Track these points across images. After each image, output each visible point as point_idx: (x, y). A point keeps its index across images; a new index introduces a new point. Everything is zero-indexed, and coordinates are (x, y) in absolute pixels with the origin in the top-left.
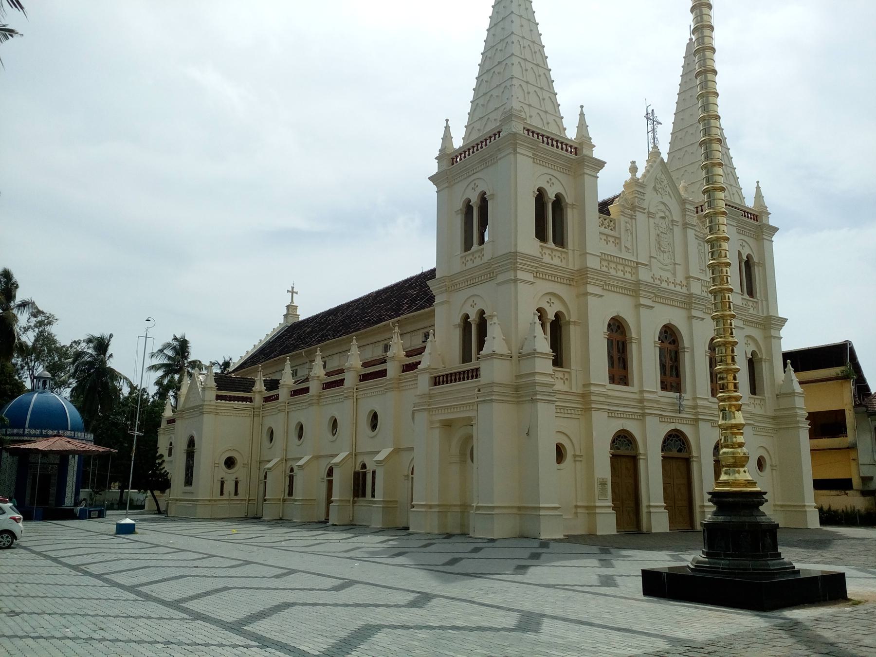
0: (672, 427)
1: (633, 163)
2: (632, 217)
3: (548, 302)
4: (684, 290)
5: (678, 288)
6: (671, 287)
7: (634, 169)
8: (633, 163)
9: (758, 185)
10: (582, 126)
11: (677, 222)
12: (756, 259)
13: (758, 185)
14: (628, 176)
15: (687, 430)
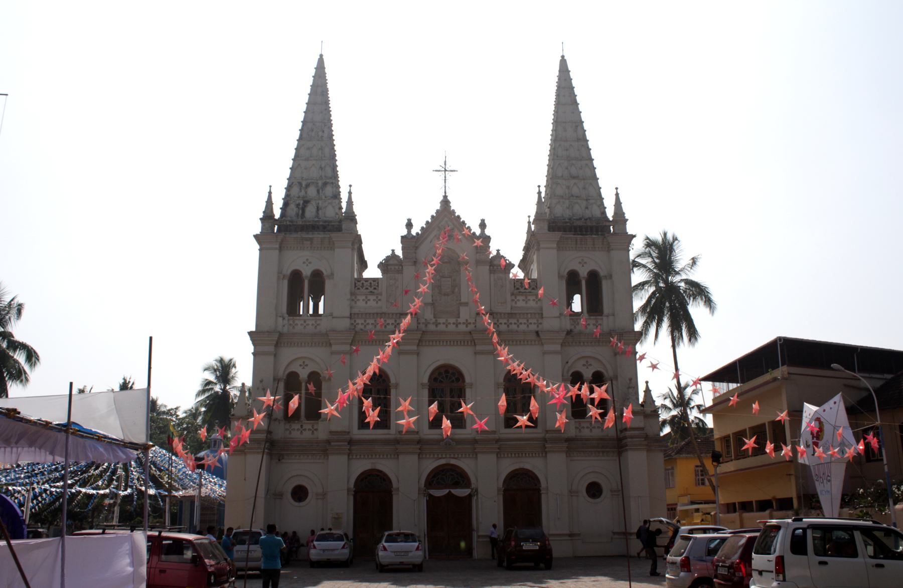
0: (443, 462)
1: (409, 220)
2: (400, 272)
3: (300, 365)
4: (471, 327)
5: (462, 328)
6: (452, 328)
7: (409, 225)
8: (409, 220)
9: (617, 192)
10: (350, 203)
11: (467, 263)
12: (602, 273)
13: (617, 192)
14: (404, 232)
15: (465, 464)
